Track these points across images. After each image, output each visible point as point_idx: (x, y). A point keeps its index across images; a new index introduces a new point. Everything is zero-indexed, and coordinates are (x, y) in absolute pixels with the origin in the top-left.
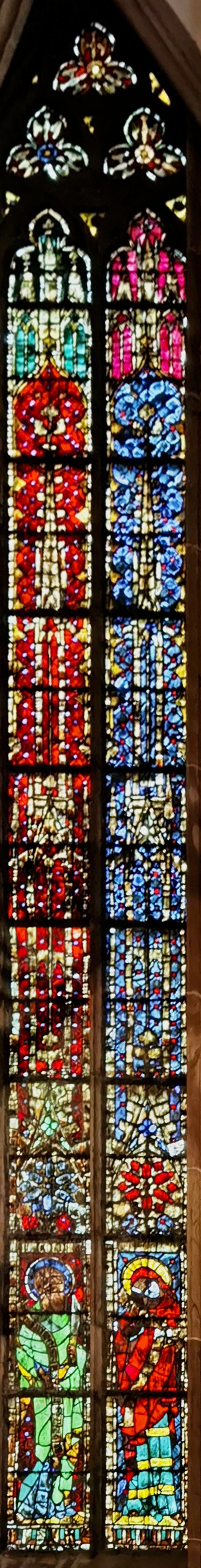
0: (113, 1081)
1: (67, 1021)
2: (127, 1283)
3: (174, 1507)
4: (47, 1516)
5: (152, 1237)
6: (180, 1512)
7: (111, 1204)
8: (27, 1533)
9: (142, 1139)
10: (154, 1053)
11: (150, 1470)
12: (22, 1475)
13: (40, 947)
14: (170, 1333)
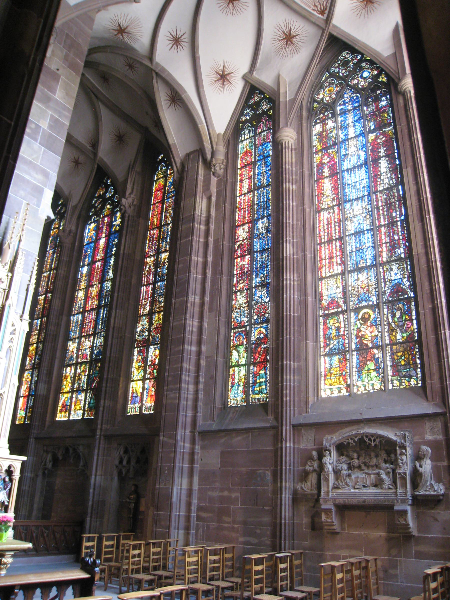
0: (254, 288)
1: (245, 277)
2: (256, 335)
3: (265, 392)
4: (237, 397)
5: (262, 323)
6: (267, 393)
7: (253, 317)
8: (232, 402)
9: (260, 299)
10: (263, 279)
11: (260, 382)
12: (232, 387)
13: (240, 262)
14: (265, 346)
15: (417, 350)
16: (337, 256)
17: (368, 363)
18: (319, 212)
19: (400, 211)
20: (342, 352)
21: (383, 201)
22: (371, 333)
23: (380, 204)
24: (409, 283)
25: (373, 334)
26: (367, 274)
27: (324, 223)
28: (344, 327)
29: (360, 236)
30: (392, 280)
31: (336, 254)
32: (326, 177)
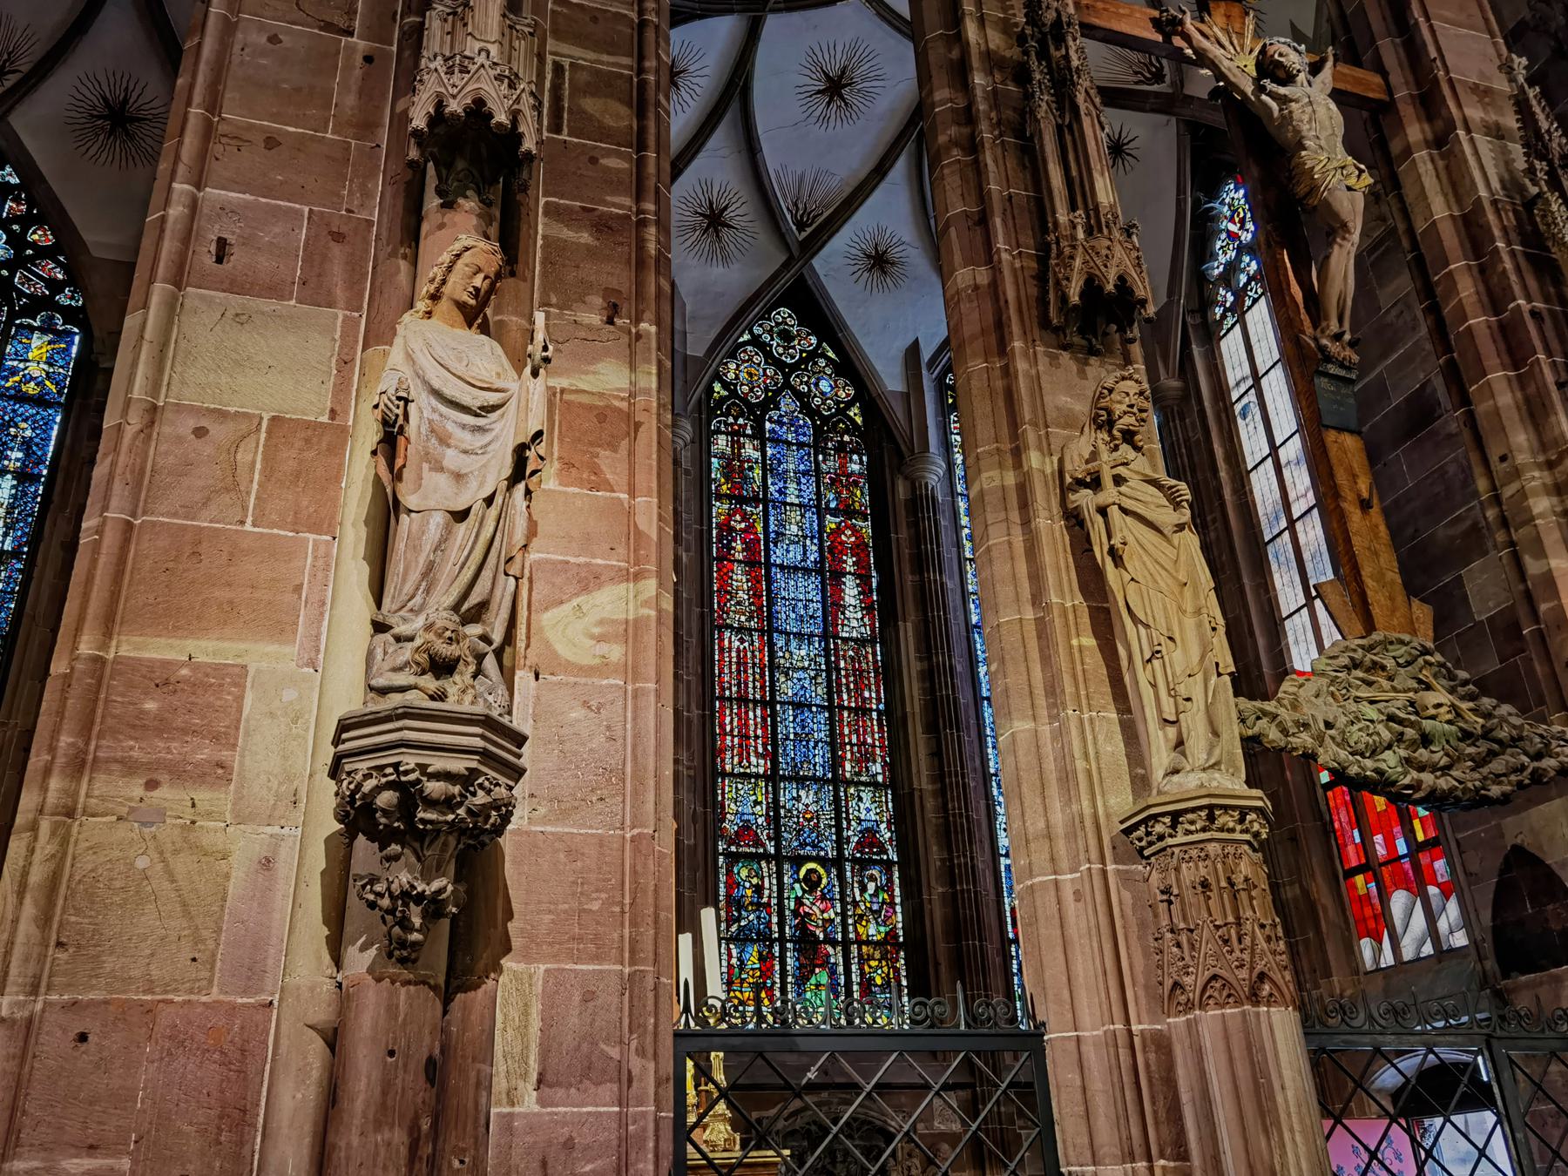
15: (903, 962)
16: (757, 737)
17: (817, 970)
18: (720, 627)
19: (878, 692)
20: (764, 938)
21: (849, 660)
22: (823, 912)
23: (842, 664)
24: (889, 834)
25: (826, 916)
26: (816, 793)
27: (730, 657)
28: (770, 889)
29: (803, 712)
30: (861, 820)
31: (755, 731)
32: (739, 562)
